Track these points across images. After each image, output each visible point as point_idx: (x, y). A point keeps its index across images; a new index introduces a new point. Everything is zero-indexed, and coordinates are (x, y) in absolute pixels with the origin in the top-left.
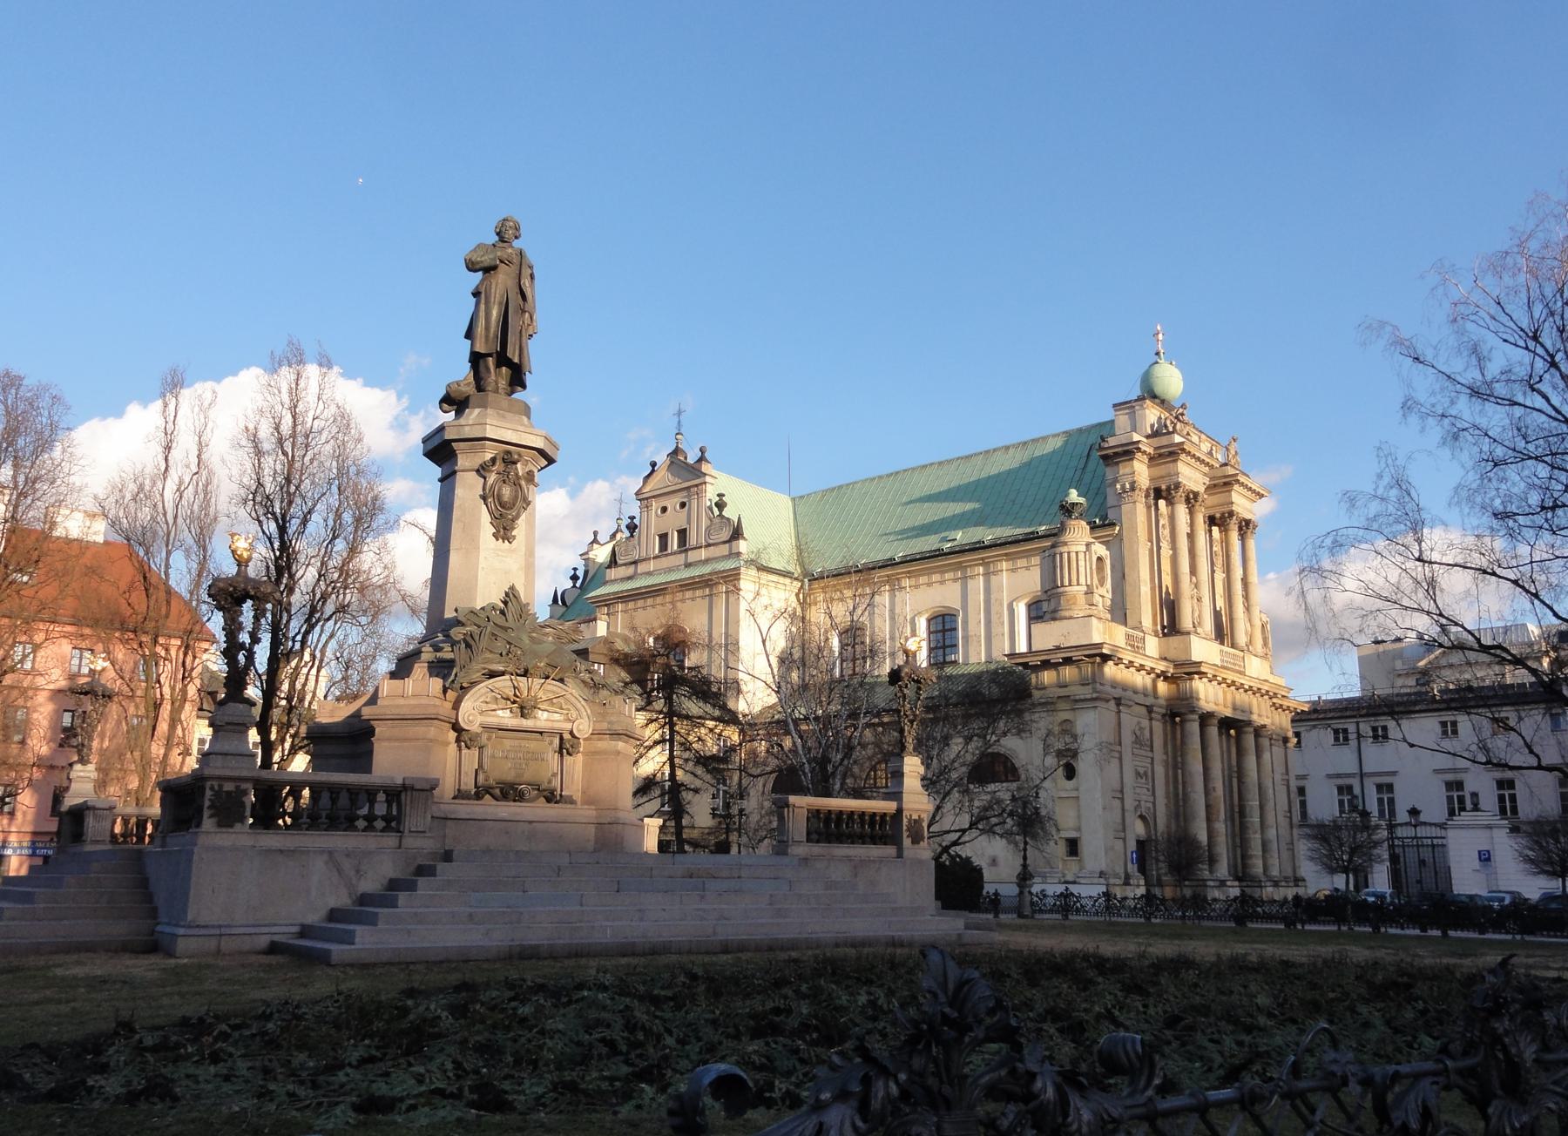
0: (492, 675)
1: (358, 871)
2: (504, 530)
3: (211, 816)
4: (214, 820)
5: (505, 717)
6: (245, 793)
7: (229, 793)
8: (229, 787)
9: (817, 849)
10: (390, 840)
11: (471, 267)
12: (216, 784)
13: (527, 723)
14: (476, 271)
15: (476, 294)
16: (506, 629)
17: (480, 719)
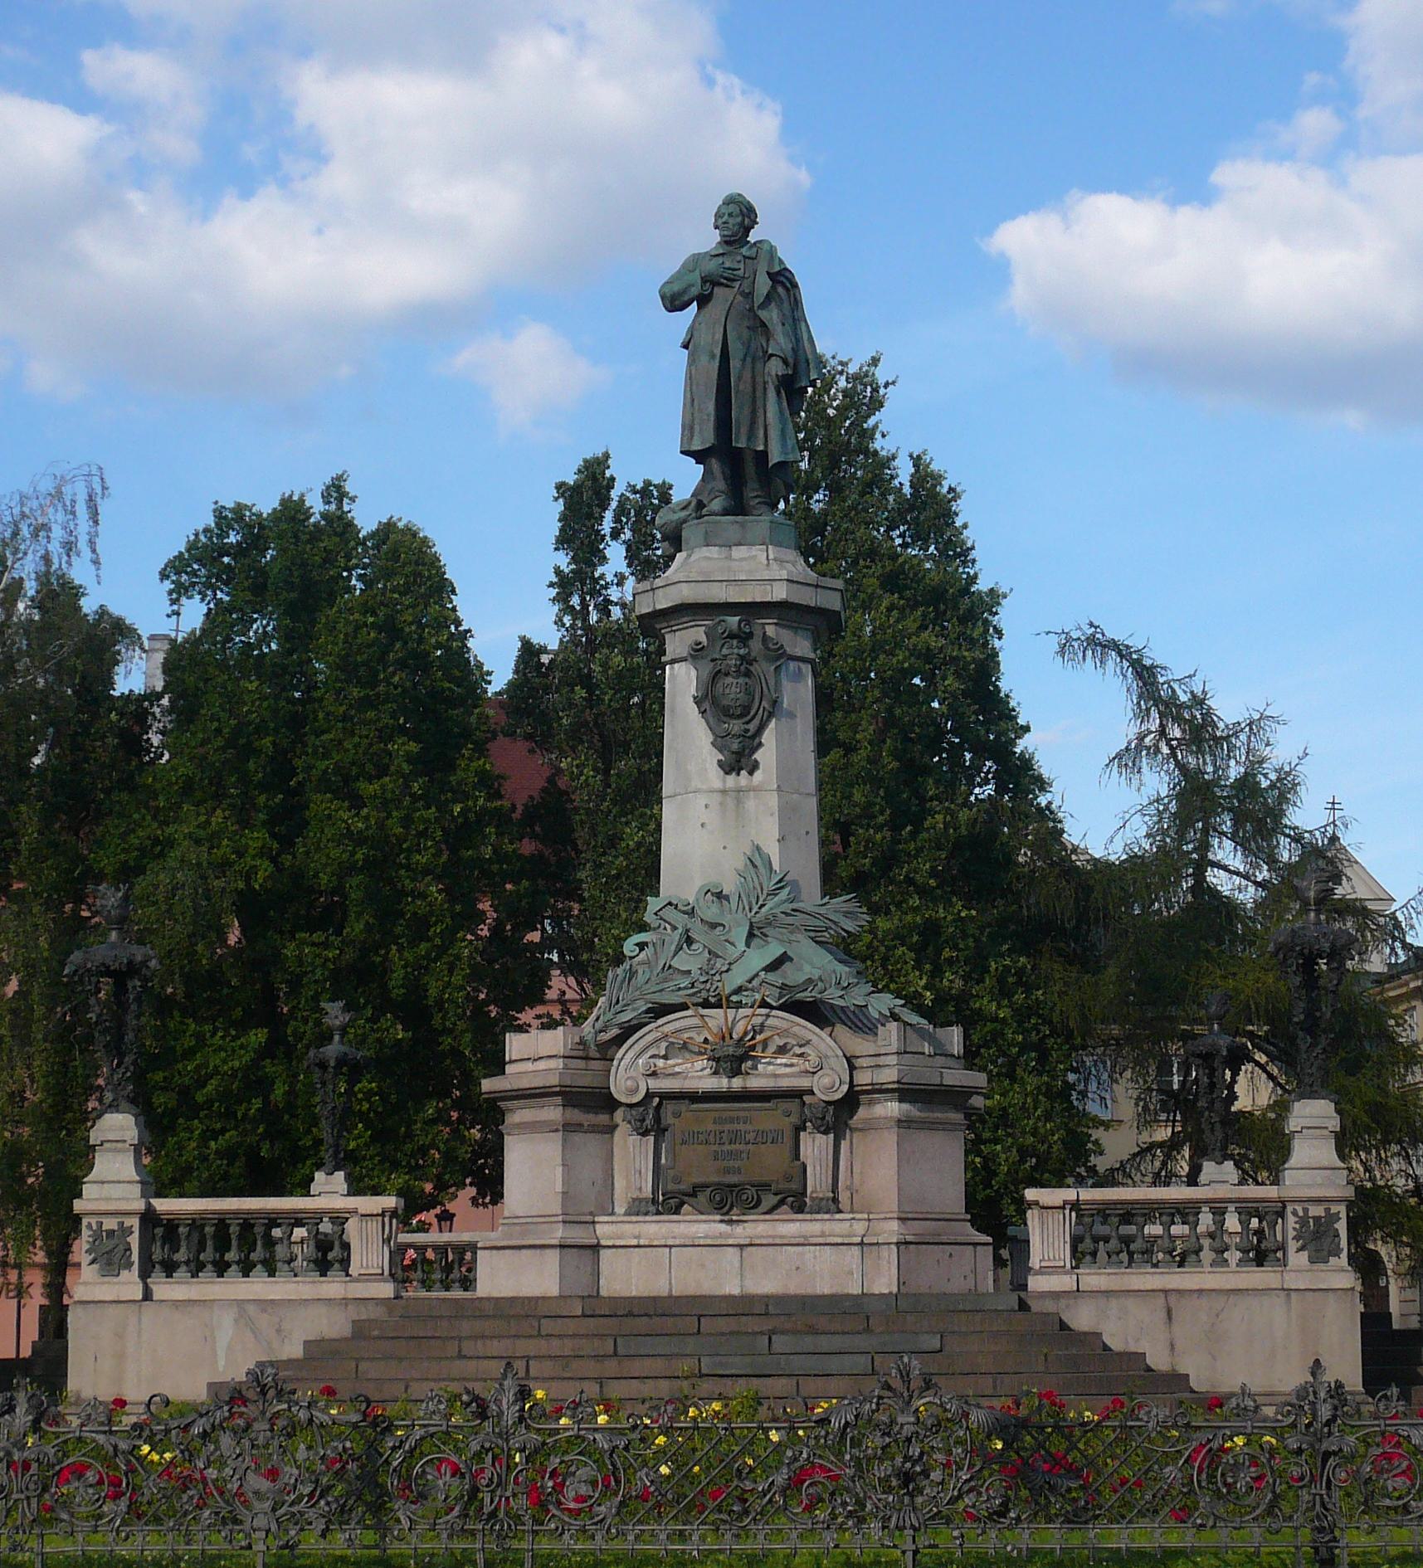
0: (661, 1011)
1: (279, 1331)
2: (739, 758)
3: (92, 1262)
4: (95, 1266)
5: (699, 1075)
6: (126, 1231)
7: (111, 1233)
8: (110, 1224)
9: (1094, 1278)
10: (333, 1287)
11: (674, 302)
12: (94, 1221)
13: (737, 1083)
14: (682, 308)
15: (686, 346)
16: (713, 926)
17: (655, 1084)
